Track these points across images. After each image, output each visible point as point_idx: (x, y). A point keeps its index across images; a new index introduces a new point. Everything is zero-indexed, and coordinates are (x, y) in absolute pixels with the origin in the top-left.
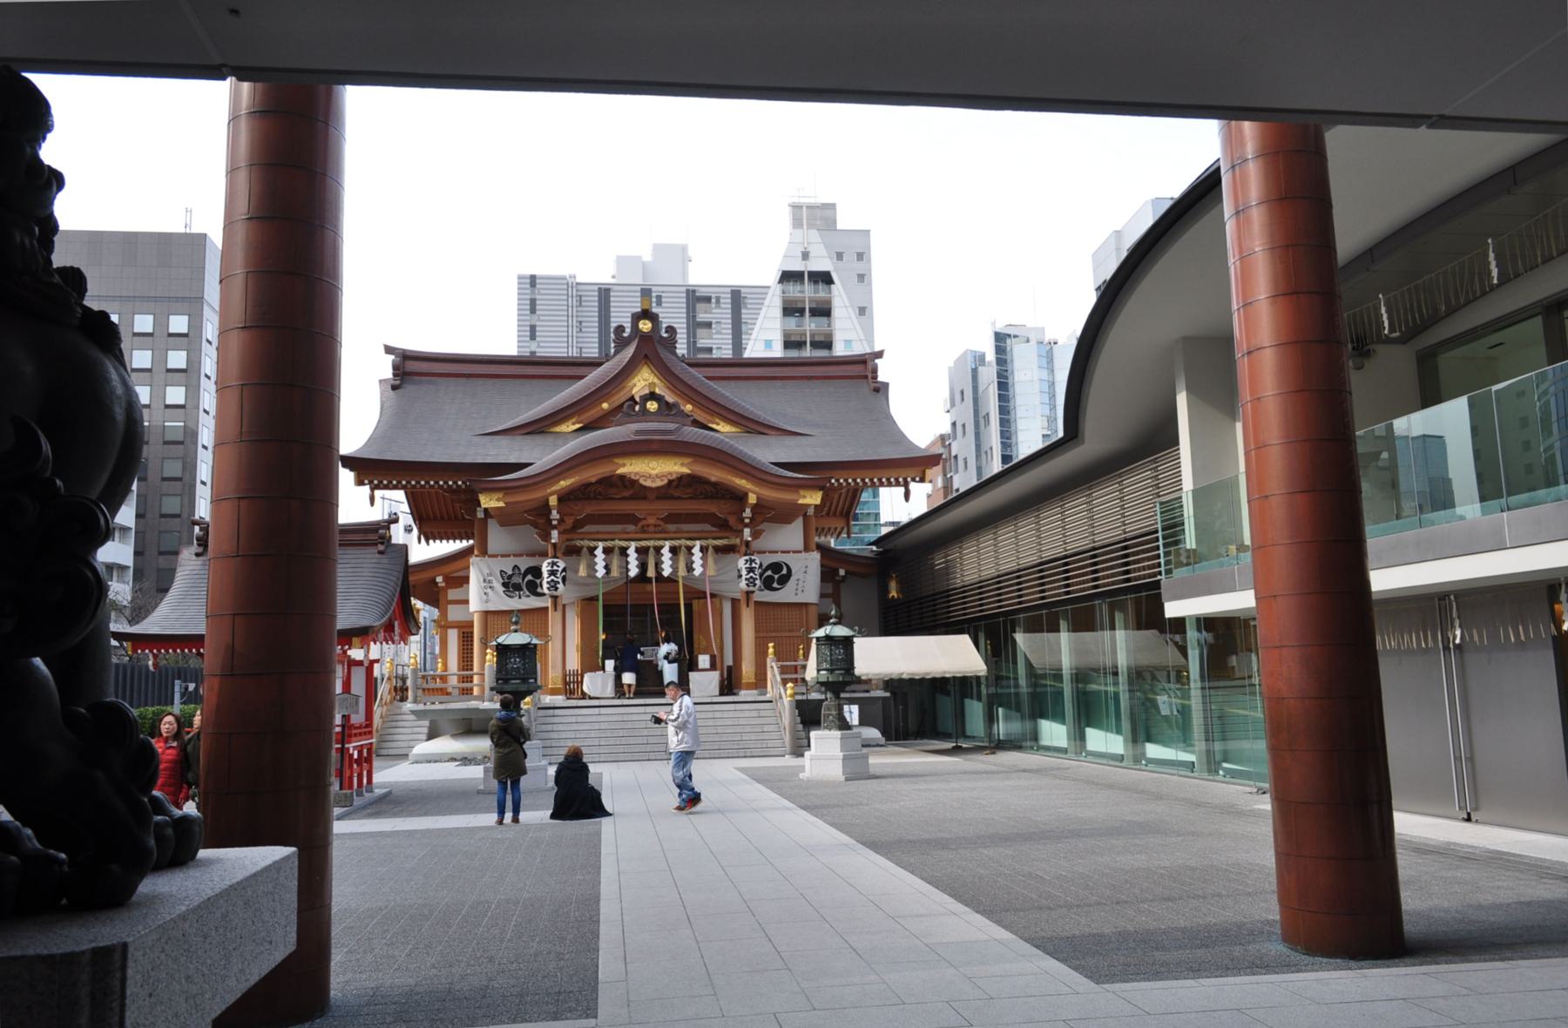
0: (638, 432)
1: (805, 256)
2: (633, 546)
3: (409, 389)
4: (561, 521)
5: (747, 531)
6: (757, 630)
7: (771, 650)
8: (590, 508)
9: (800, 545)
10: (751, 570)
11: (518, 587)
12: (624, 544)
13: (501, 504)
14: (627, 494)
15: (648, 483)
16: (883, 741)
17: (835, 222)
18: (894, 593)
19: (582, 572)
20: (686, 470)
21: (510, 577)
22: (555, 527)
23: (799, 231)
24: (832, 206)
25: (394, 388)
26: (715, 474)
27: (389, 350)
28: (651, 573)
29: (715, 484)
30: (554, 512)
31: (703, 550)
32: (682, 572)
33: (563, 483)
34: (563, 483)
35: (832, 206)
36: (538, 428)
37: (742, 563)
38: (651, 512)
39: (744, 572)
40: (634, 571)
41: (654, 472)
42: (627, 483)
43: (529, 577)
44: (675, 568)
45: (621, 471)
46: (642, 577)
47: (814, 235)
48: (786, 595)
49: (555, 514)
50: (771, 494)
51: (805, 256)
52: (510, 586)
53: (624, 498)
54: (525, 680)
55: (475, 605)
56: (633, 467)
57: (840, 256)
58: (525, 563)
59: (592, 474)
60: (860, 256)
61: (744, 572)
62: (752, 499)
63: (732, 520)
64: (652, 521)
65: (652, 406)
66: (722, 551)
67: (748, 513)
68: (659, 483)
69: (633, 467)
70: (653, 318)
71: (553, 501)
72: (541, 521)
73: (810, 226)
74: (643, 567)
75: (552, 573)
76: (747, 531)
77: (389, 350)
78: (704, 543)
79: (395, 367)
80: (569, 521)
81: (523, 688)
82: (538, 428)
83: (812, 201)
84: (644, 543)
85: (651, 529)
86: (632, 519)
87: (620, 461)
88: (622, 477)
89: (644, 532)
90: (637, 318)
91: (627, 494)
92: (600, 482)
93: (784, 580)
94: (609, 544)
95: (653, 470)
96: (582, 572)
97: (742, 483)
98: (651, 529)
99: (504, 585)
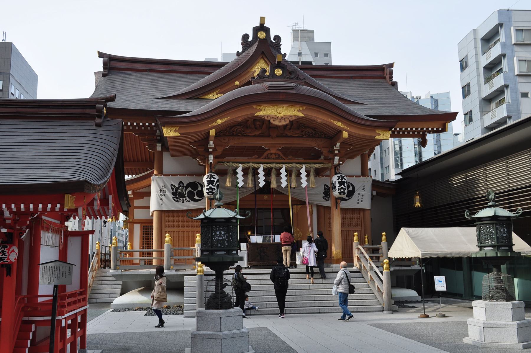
0: (270, 87)
1: (300, 54)
2: (262, 167)
3: (112, 77)
4: (214, 149)
5: (337, 159)
6: (343, 225)
7: (356, 237)
8: (234, 142)
9: (359, 172)
10: (341, 183)
11: (182, 195)
12: (255, 165)
13: (178, 134)
14: (257, 133)
15: (276, 123)
16: (419, 299)
17: (313, 39)
18: (418, 204)
19: (228, 183)
20: (301, 115)
21: (177, 189)
22: (211, 153)
23: (297, 42)
24: (312, 32)
25: (104, 75)
26: (320, 118)
27: (101, 55)
28: (273, 185)
30: (211, 143)
32: (294, 185)
33: (219, 121)
34: (219, 121)
35: (312, 32)
39: (337, 185)
40: (262, 184)
41: (280, 115)
43: (190, 189)
47: (304, 44)
48: (351, 204)
51: (300, 54)
52: (177, 195)
53: (255, 136)
54: (229, 252)
55: (154, 205)
56: (267, 112)
57: (316, 55)
58: (187, 180)
59: (239, 115)
60: (326, 55)
61: (337, 185)
62: (345, 135)
64: (273, 151)
66: (319, 173)
68: (283, 123)
69: (267, 112)
70: (267, 30)
71: (213, 133)
72: (201, 149)
73: (302, 40)
74: (268, 182)
75: (210, 182)
76: (337, 159)
77: (101, 55)
78: (308, 166)
79: (105, 64)
80: (220, 150)
81: (229, 259)
83: (302, 28)
84: (269, 165)
85: (273, 156)
87: (258, 107)
88: (261, 120)
89: (267, 158)
90: (256, 30)
91: (257, 133)
93: (351, 194)
94: (246, 165)
95: (280, 113)
96: (228, 183)
98: (273, 156)
99: (173, 194)
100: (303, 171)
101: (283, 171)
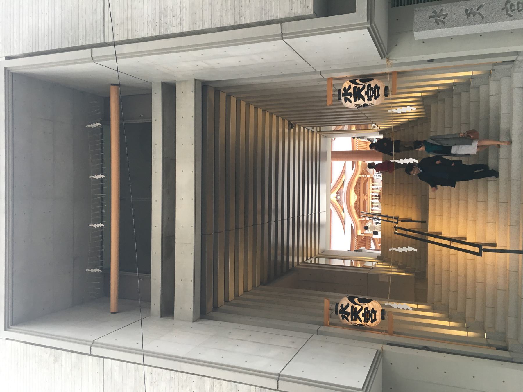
26: (354, 184)
29: (357, 183)
31: (373, 185)
36: (343, 222)
37: (375, 178)
38: (363, 197)
42: (356, 203)
44: (376, 193)
45: (353, 205)
46: (379, 199)
49: (363, 219)
50: (359, 171)
59: (354, 211)
62: (360, 176)
63: (366, 179)
65: (339, 197)
66: (373, 182)
67: (364, 176)
71: (360, 219)
72: (364, 222)
76: (368, 176)
82: (343, 222)
86: (365, 202)
88: (355, 204)
92: (355, 209)
95: (353, 197)
97: (356, 179)
100: (373, 194)
101: (373, 194)
